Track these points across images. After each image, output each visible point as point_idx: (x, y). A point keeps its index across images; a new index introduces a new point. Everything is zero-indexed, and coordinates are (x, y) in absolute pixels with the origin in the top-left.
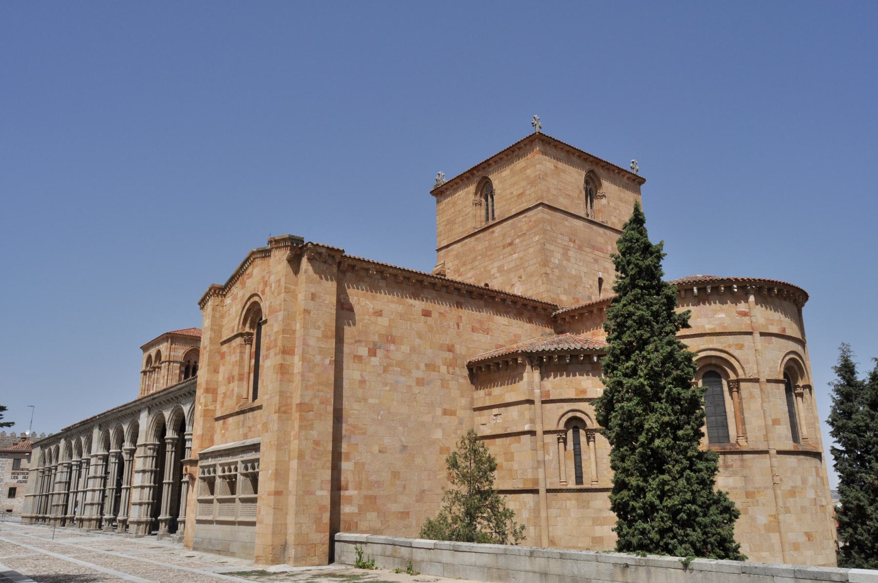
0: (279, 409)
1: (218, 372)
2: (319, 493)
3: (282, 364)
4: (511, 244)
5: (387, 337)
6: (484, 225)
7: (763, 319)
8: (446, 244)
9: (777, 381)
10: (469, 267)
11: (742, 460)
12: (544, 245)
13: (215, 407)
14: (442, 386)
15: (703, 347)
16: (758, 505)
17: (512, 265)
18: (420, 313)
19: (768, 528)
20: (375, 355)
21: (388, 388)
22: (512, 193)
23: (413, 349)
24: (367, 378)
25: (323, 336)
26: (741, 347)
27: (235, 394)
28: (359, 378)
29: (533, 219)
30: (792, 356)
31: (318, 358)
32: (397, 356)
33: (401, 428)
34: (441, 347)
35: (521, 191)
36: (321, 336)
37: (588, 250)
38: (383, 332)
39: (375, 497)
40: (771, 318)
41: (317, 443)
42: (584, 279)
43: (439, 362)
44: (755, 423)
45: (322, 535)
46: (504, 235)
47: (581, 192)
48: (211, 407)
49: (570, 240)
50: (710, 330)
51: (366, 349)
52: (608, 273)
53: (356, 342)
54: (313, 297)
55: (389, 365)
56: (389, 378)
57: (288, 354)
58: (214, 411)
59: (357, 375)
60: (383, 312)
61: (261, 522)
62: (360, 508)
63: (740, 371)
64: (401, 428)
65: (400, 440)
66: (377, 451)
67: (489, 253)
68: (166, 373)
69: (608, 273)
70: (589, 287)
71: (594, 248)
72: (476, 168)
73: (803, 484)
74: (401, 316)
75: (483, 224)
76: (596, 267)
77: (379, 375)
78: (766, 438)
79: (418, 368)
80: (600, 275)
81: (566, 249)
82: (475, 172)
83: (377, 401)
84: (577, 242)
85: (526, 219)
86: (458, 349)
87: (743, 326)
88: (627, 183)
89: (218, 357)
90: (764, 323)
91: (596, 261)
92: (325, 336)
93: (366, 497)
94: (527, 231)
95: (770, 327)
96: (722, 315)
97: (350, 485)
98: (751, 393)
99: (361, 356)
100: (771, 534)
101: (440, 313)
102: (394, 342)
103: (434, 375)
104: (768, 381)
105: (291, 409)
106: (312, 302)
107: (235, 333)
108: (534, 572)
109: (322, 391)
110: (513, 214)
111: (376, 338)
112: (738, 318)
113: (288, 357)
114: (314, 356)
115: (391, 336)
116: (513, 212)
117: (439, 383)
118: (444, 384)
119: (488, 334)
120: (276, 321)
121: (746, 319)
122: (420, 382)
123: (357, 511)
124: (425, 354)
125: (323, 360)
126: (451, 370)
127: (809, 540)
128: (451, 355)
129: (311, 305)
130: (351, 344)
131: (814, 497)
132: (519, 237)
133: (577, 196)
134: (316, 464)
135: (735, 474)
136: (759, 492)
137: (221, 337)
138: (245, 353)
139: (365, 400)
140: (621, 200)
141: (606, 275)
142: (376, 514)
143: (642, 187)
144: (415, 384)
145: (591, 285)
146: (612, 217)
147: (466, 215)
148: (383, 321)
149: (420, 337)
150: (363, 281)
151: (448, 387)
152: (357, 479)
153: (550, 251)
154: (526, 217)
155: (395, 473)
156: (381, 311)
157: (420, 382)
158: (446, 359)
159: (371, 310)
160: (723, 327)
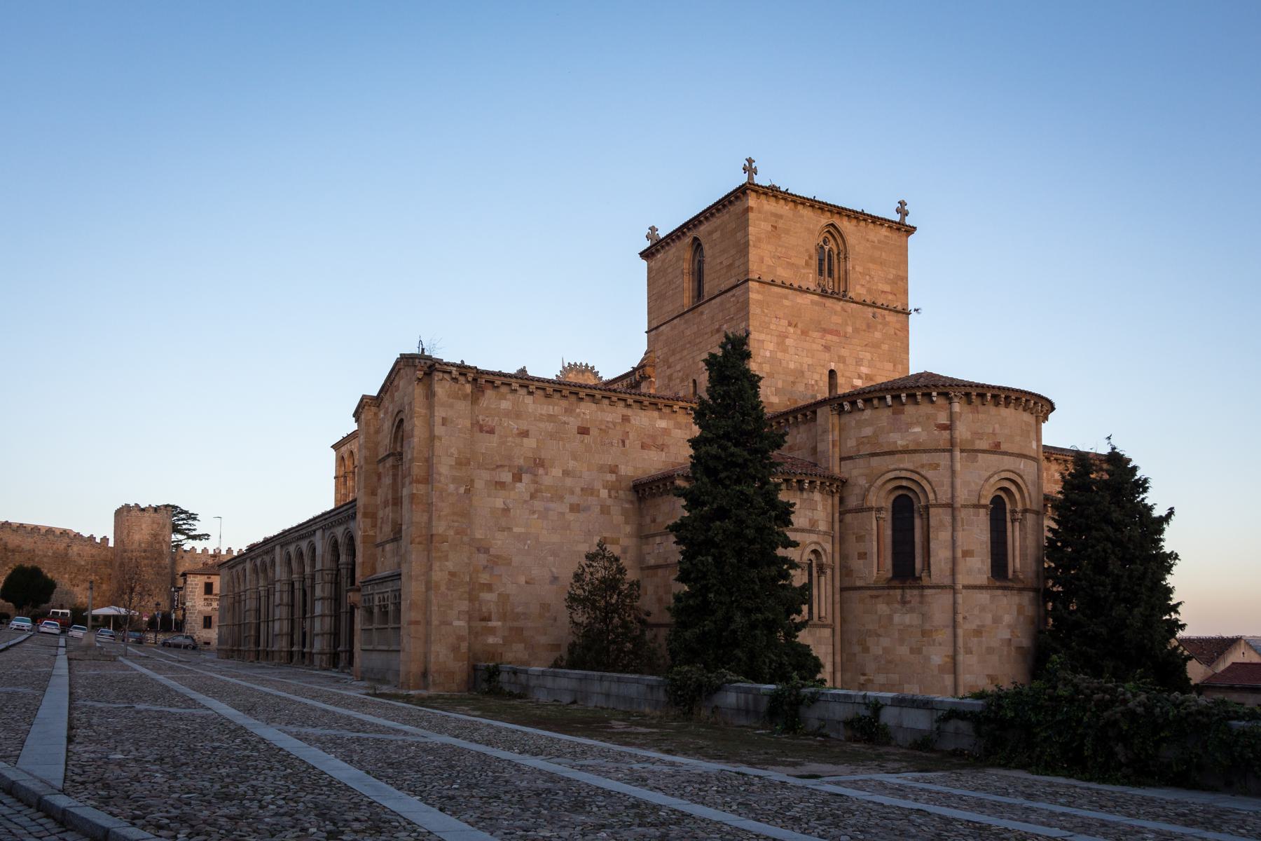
1: (376, 495)
2: (456, 623)
5: (535, 460)
7: (969, 433)
8: (656, 326)
10: (678, 356)
13: (375, 533)
14: (602, 512)
15: (892, 467)
16: (934, 645)
18: (575, 431)
19: (942, 669)
20: (520, 480)
21: (536, 516)
22: (721, 263)
23: (566, 473)
24: (511, 506)
25: (456, 464)
26: (936, 467)
27: (390, 520)
28: (502, 506)
29: (741, 300)
30: (900, 492)
31: (452, 487)
32: (547, 481)
34: (601, 469)
35: (730, 261)
36: (454, 464)
37: (816, 334)
39: (522, 629)
40: (980, 431)
41: (452, 574)
42: (807, 374)
43: (598, 485)
44: (940, 554)
45: (461, 664)
46: (713, 318)
47: (810, 257)
49: (790, 324)
50: (901, 446)
51: (510, 475)
52: (844, 362)
55: (537, 491)
56: (537, 504)
59: (499, 503)
60: (530, 432)
61: (404, 651)
62: (504, 638)
63: (931, 496)
64: (552, 558)
65: (550, 570)
66: (524, 583)
67: (698, 341)
69: (844, 362)
71: (825, 331)
72: (686, 225)
74: (552, 436)
76: (827, 356)
77: (526, 502)
78: (953, 572)
79: (572, 493)
80: (833, 366)
81: (783, 336)
82: (685, 230)
83: (523, 530)
84: (800, 325)
85: (734, 299)
87: (941, 442)
88: (886, 236)
90: (969, 438)
91: (827, 348)
93: (511, 629)
95: (977, 442)
96: (917, 429)
97: (493, 617)
98: (941, 521)
101: (601, 429)
102: (543, 466)
103: (592, 500)
104: (964, 506)
107: (388, 452)
108: (602, 694)
109: (457, 521)
111: (521, 462)
112: (936, 432)
114: (447, 485)
115: (540, 459)
117: (597, 509)
118: (605, 510)
119: (662, 450)
121: (946, 434)
122: (575, 508)
123: (501, 642)
124: (581, 477)
125: (457, 489)
126: (613, 493)
128: (614, 476)
130: (493, 469)
131: (1009, 637)
132: (727, 322)
133: (804, 264)
134: (452, 595)
135: (912, 610)
136: (936, 630)
137: (377, 457)
139: (510, 529)
140: (873, 260)
141: (841, 365)
142: (523, 645)
143: (911, 238)
144: (568, 511)
145: (816, 381)
146: (858, 287)
147: (676, 288)
148: (530, 443)
149: (575, 458)
150: (505, 399)
151: (609, 513)
152: (501, 611)
153: (758, 340)
154: (734, 295)
155: (544, 604)
156: (527, 431)
157: (575, 508)
158: (607, 481)
159: (515, 431)
160: (918, 444)
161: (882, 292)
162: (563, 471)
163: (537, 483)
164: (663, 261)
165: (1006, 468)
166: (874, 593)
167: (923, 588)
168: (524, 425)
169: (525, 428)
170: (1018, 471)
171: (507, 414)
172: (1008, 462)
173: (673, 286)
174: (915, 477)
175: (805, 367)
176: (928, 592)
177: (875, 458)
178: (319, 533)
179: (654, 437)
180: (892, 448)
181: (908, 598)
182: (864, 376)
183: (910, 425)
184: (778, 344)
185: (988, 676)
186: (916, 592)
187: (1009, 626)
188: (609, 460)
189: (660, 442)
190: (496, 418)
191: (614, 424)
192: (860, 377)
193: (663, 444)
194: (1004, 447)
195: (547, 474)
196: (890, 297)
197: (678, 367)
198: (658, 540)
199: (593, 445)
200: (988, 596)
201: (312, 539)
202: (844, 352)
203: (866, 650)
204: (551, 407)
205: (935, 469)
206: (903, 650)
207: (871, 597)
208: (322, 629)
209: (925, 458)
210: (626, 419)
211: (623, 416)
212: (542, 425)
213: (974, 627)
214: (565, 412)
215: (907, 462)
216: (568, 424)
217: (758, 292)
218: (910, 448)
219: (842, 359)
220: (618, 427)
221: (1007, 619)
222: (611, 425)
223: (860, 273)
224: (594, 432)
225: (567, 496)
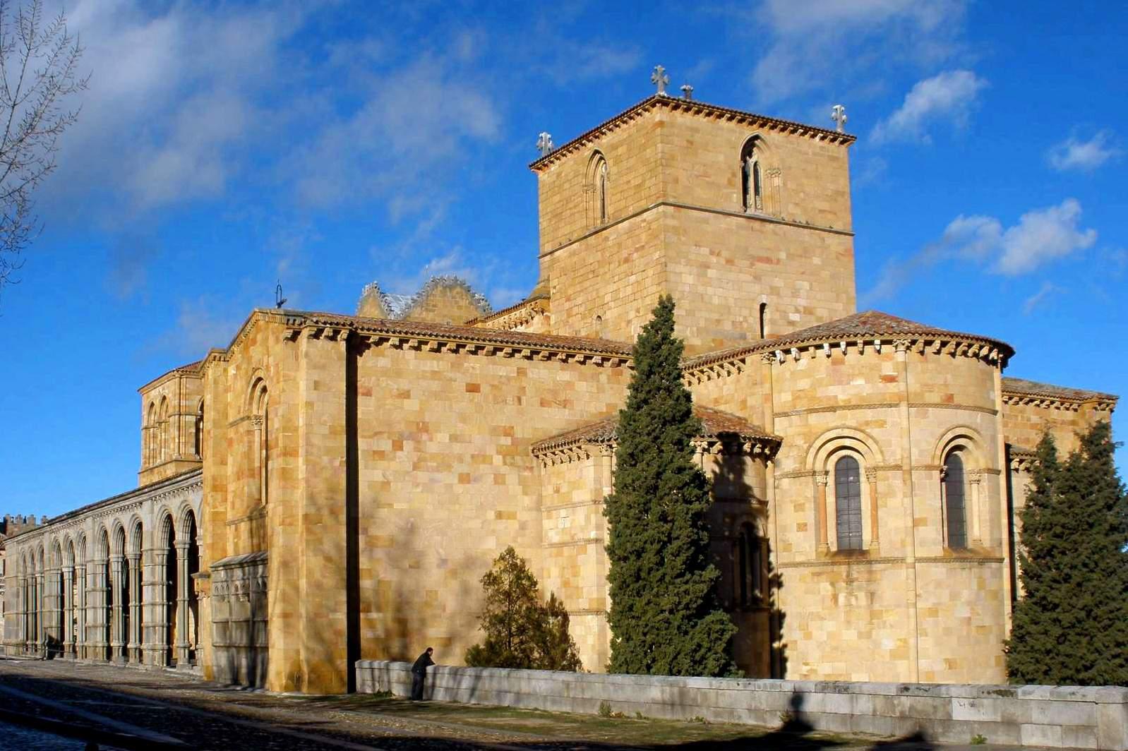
0: (283, 521)
1: (226, 464)
3: (283, 468)
4: (627, 260)
6: (599, 224)
9: (929, 468)
11: (870, 572)
12: (666, 266)
13: (226, 508)
14: (496, 482)
17: (629, 290)
20: (401, 448)
21: (419, 490)
22: (629, 182)
23: (454, 438)
24: (391, 478)
25: (331, 433)
26: (882, 424)
28: (381, 479)
31: (325, 459)
33: (439, 538)
34: (495, 431)
35: (638, 181)
38: (412, 419)
40: (930, 382)
43: (491, 450)
47: (734, 175)
48: (221, 509)
49: (712, 253)
52: (778, 294)
53: (376, 434)
54: (317, 385)
55: (420, 460)
56: (422, 476)
57: (291, 455)
58: (225, 513)
64: (439, 538)
65: (438, 553)
68: (177, 433)
69: (778, 294)
70: (741, 319)
73: (950, 600)
74: (436, 395)
75: (599, 222)
76: (757, 288)
86: (519, 434)
89: (225, 444)
90: (919, 391)
91: (757, 278)
92: (333, 432)
94: (647, 243)
95: (927, 394)
96: (860, 382)
99: (384, 451)
100: (899, 662)
101: (493, 386)
102: (427, 431)
103: (483, 468)
105: (298, 520)
106: (315, 392)
107: (242, 415)
110: (631, 214)
113: (291, 459)
114: (320, 458)
115: (423, 423)
116: (631, 211)
118: (499, 479)
119: (565, 407)
120: (276, 415)
124: (470, 442)
125: (331, 461)
126: (509, 460)
127: (950, 668)
128: (509, 439)
129: (314, 394)
130: (370, 437)
131: (969, 615)
132: (637, 250)
138: (254, 442)
141: (774, 298)
144: (456, 481)
145: (745, 317)
147: (575, 207)
148: (411, 405)
150: (383, 356)
151: (504, 483)
156: (409, 391)
157: (465, 479)
160: (862, 398)
161: (821, 211)
162: (450, 435)
163: (419, 450)
164: (559, 175)
165: (961, 423)
166: (817, 569)
167: (870, 562)
168: (404, 384)
169: (406, 388)
170: (974, 427)
171: (385, 372)
172: (963, 416)
173: (571, 205)
174: (859, 435)
175: (731, 301)
176: (877, 567)
177: (814, 414)
178: (147, 505)
179: (555, 393)
180: (832, 403)
181: (855, 575)
182: (802, 310)
183: (851, 377)
184: (699, 275)
185: (947, 660)
186: (862, 567)
187: (969, 603)
188: (502, 421)
189: (562, 397)
190: (373, 378)
191: (509, 379)
192: (797, 311)
193: (565, 401)
194: (957, 400)
195: (431, 440)
196: (830, 216)
197: (580, 300)
198: (563, 513)
199: (484, 405)
200: (944, 570)
201: (138, 511)
202: (778, 282)
203: (808, 636)
204: (435, 362)
205: (882, 426)
206: (850, 635)
207: (814, 574)
208: (152, 622)
209: (869, 414)
210: (521, 372)
211: (518, 369)
212: (424, 383)
213: (929, 605)
214: (452, 366)
215: (852, 418)
216: (455, 381)
217: (673, 217)
218: (852, 403)
219: (774, 291)
220: (513, 383)
221: (966, 595)
222: (503, 380)
223: (793, 190)
224: (485, 389)
225: (455, 464)
